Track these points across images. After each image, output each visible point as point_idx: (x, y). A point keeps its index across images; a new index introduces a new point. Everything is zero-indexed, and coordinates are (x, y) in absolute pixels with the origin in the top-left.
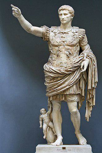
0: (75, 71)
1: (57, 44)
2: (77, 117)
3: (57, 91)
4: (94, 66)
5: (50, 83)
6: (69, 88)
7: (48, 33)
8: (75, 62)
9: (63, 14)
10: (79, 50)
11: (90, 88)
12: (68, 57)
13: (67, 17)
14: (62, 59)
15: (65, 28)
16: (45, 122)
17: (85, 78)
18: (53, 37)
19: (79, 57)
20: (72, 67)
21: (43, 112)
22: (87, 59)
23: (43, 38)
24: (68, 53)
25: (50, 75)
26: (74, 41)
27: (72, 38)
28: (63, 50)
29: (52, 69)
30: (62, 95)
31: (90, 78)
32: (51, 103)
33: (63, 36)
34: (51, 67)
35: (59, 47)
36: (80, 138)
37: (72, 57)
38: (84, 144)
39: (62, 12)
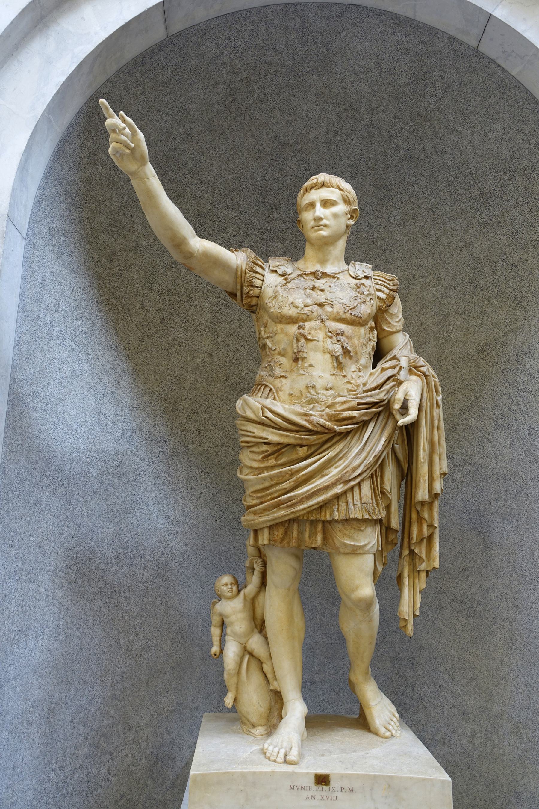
0: (364, 424)
1: (292, 312)
2: (371, 621)
3: (291, 503)
4: (437, 411)
5: (261, 470)
6: (345, 493)
7: (256, 272)
8: (368, 387)
9: (318, 205)
10: (375, 345)
11: (426, 497)
12: (340, 366)
13: (335, 216)
14: (316, 373)
15: (323, 262)
16: (235, 634)
17: (400, 456)
18: (280, 290)
19: (383, 370)
20: (359, 404)
21: (225, 588)
22: (414, 378)
23: (239, 294)
24: (338, 348)
25: (264, 434)
26: (363, 306)
27: (353, 293)
28: (320, 335)
29: (274, 409)
30: (314, 523)
31: (422, 455)
32: (260, 554)
33: (317, 285)
34: (268, 402)
35: (301, 324)
36: (372, 703)
37: (353, 367)
38: (394, 732)
39: (315, 195)
